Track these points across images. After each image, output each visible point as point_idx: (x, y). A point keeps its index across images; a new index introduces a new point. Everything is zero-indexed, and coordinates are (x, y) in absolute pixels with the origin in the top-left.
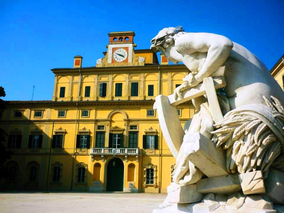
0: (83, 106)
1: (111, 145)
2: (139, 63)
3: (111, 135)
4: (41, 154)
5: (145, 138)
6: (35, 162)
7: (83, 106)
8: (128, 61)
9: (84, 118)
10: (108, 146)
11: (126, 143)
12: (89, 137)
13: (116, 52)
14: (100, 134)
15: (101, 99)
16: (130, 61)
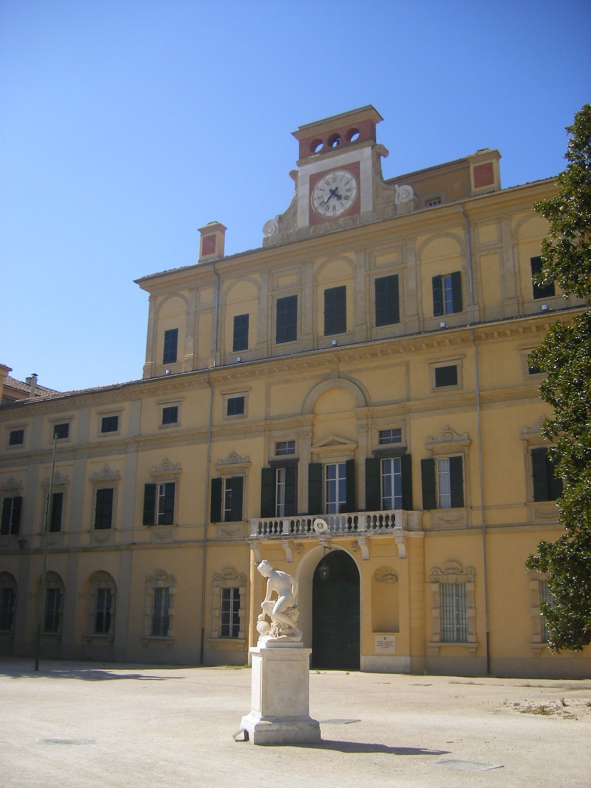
2: (395, 206)
4: (118, 548)
6: (102, 575)
8: (359, 208)
10: (306, 511)
13: (321, 184)
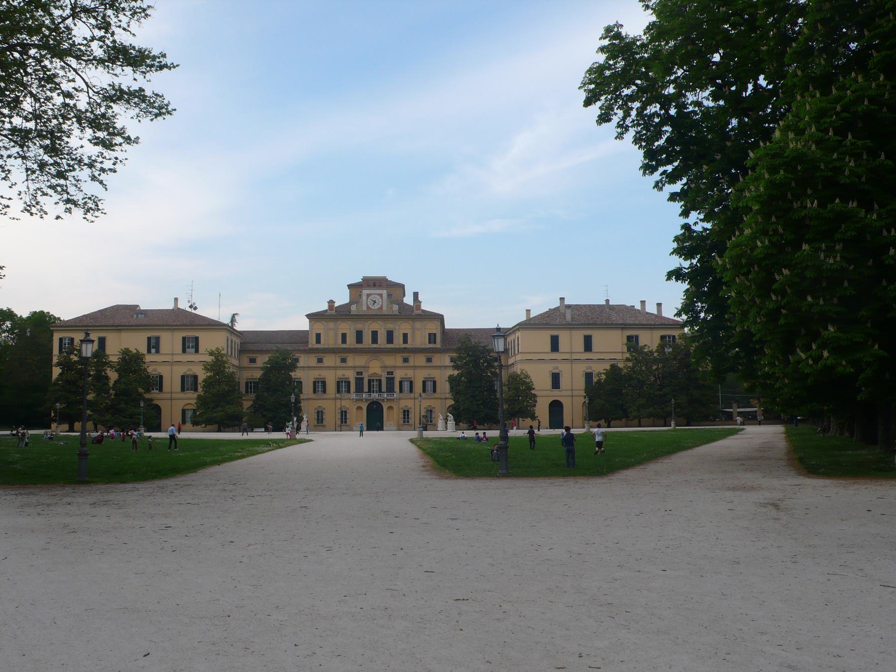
0: (342, 353)
1: (369, 391)
3: (370, 381)
5: (401, 382)
7: (342, 353)
9: (343, 365)
11: (384, 388)
12: (349, 383)
14: (359, 381)
15: (359, 346)
16: (385, 308)
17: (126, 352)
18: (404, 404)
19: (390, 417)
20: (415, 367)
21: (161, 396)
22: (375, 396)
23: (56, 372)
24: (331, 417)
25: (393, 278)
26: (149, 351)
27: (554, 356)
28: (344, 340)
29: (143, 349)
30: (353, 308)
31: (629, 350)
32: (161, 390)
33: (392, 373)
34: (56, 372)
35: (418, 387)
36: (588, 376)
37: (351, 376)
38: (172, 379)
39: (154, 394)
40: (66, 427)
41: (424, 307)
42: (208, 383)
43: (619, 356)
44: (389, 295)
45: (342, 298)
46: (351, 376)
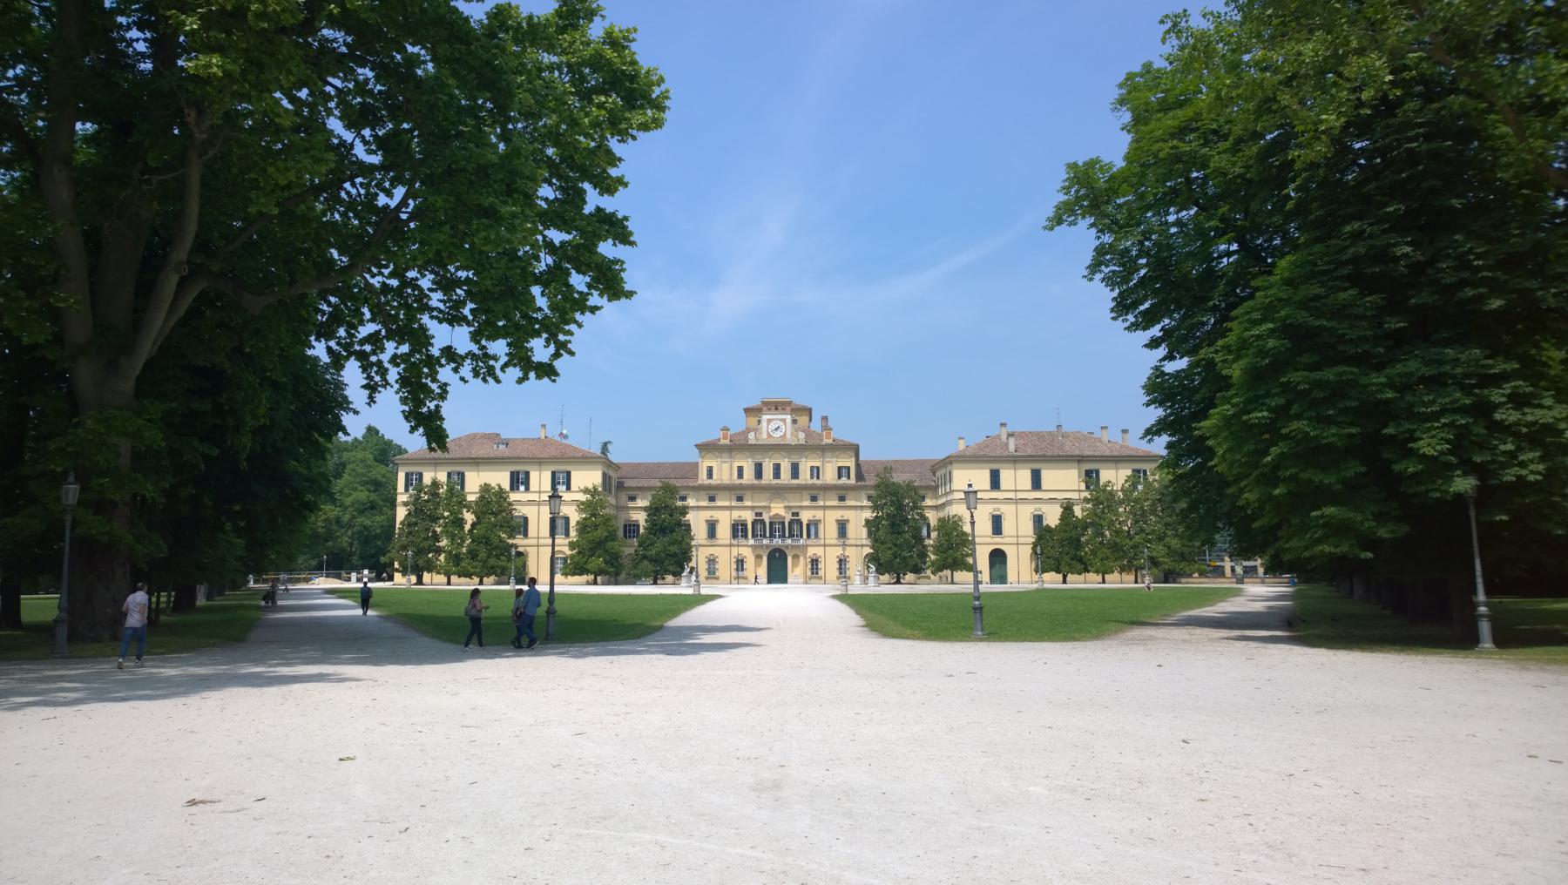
0: (738, 493)
7: (738, 493)
12: (744, 525)
17: (486, 488)
18: (811, 552)
19: (796, 571)
20: (825, 508)
21: (526, 542)
22: (777, 542)
23: (401, 513)
24: (725, 567)
25: (800, 401)
26: (512, 489)
27: (995, 495)
28: (740, 475)
29: (506, 486)
30: (751, 436)
31: (1087, 487)
32: (526, 535)
33: (796, 514)
34: (401, 513)
35: (830, 531)
36: (1038, 519)
37: (749, 517)
38: (538, 521)
39: (519, 540)
40: (414, 579)
41: (834, 434)
42: (583, 527)
43: (1074, 496)
44: (794, 422)
45: (738, 423)
46: (749, 517)
